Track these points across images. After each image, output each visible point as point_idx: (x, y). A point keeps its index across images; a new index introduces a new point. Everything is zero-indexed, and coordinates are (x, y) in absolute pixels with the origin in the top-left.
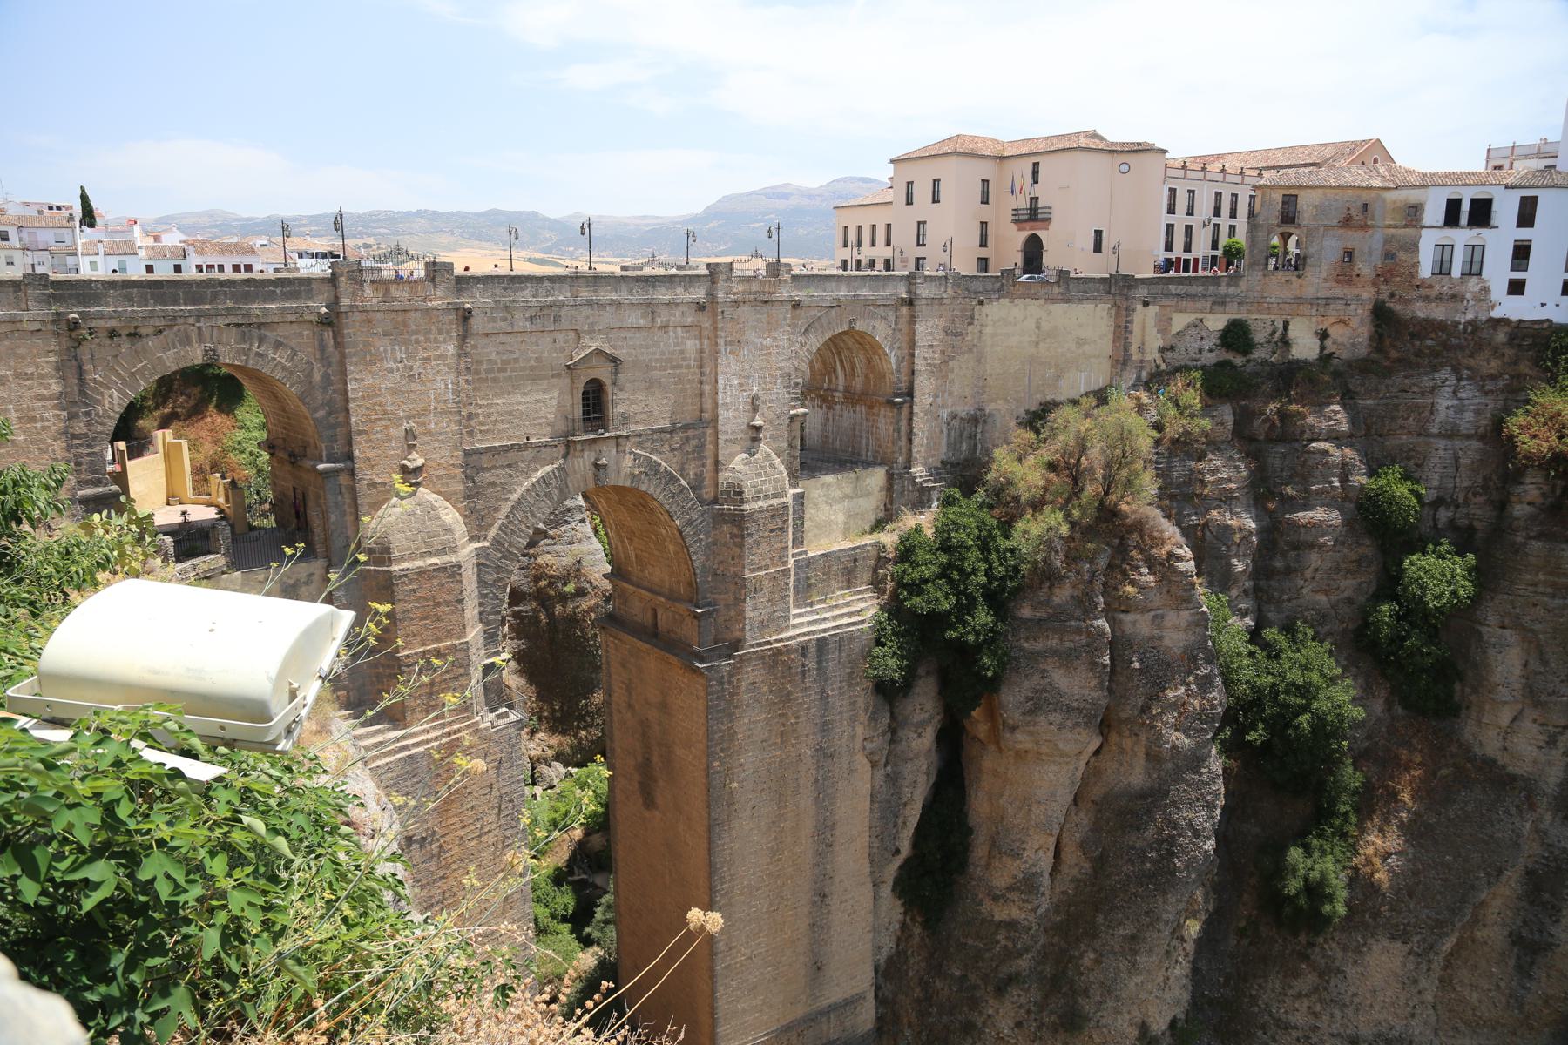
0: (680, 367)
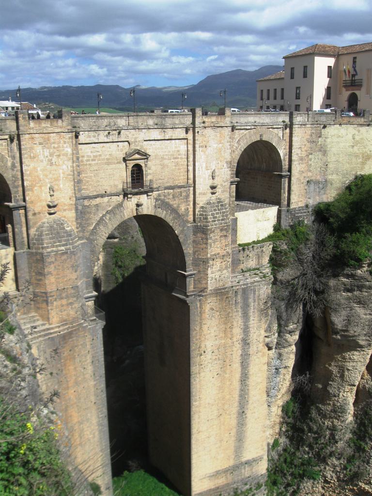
0: (178, 158)
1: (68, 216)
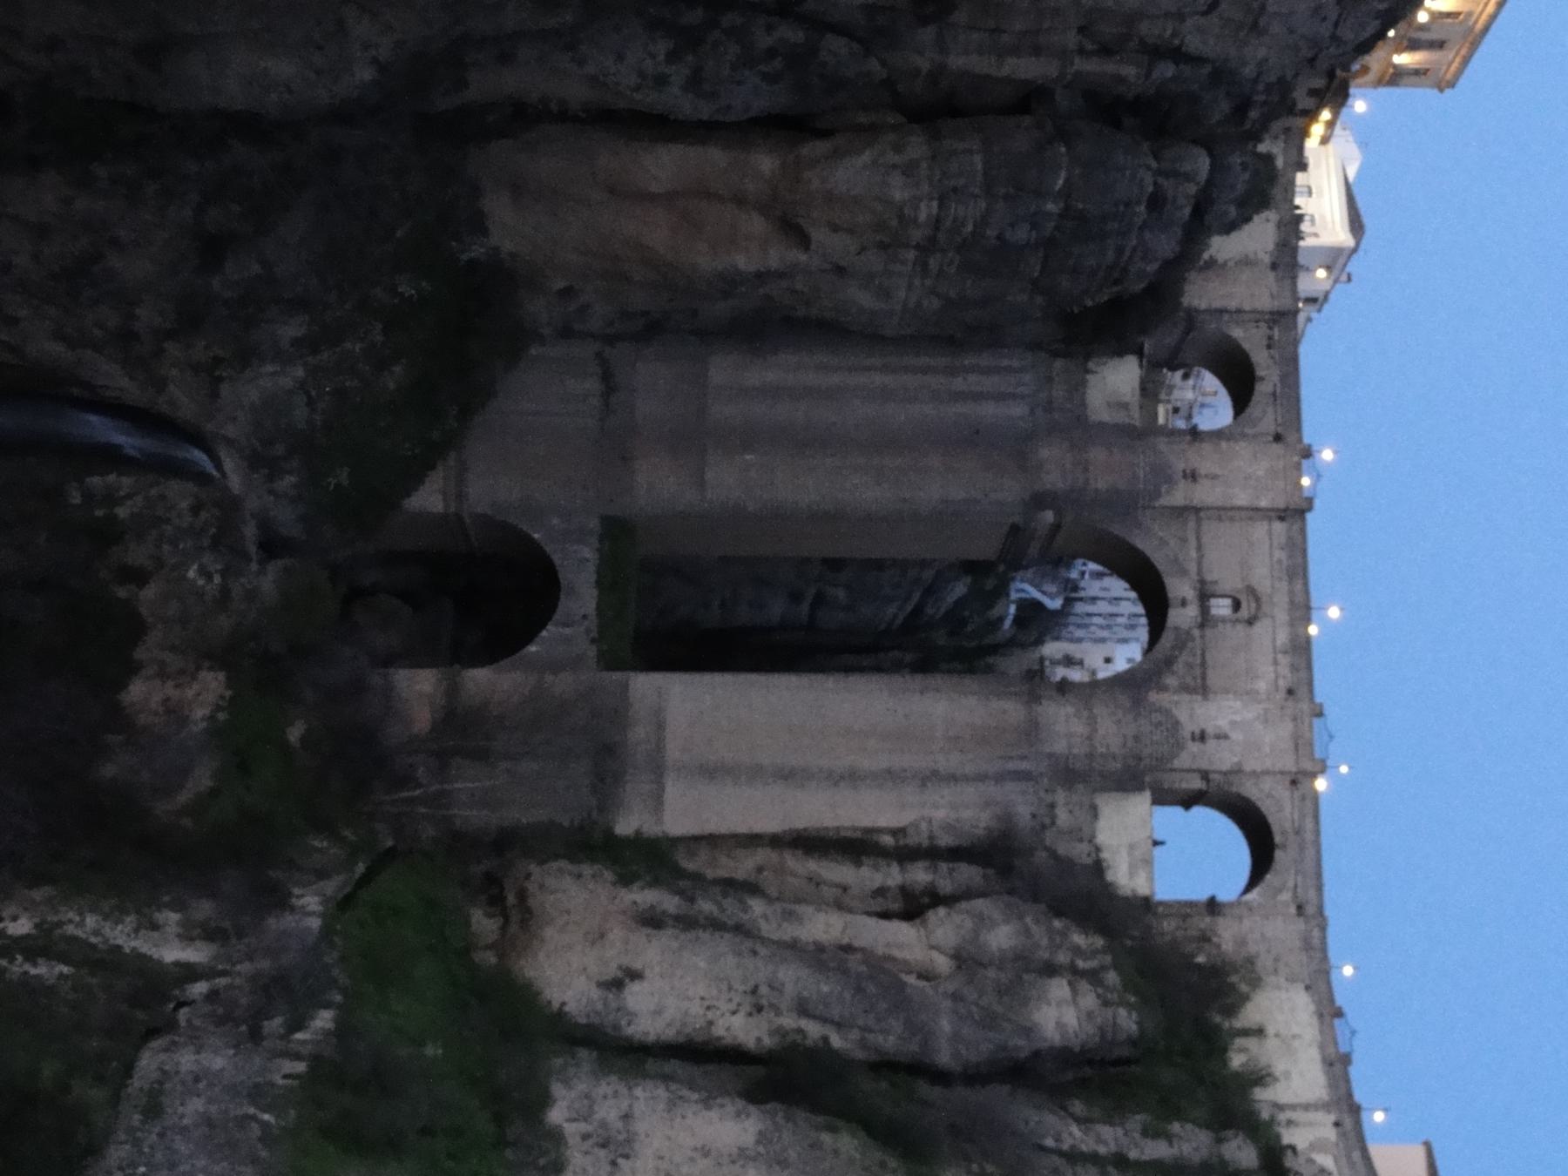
1: (1178, 496)
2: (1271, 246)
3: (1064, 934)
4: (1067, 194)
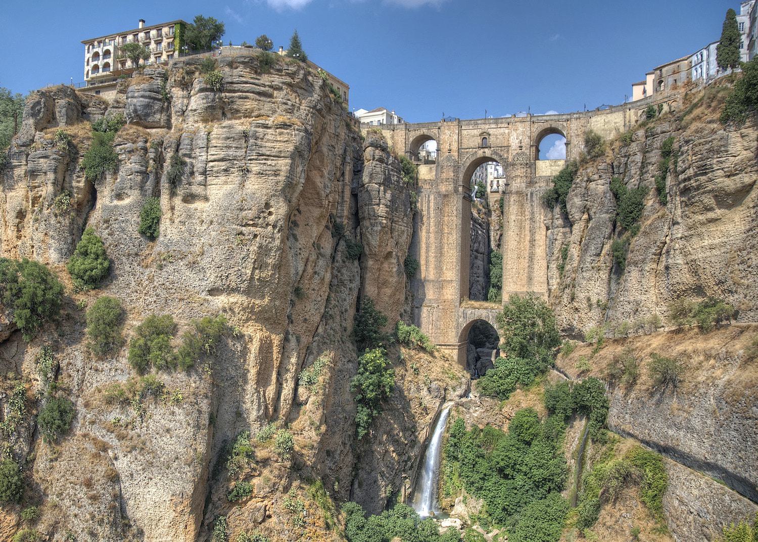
2: (389, 131)
3: (578, 183)
4: (380, 184)
